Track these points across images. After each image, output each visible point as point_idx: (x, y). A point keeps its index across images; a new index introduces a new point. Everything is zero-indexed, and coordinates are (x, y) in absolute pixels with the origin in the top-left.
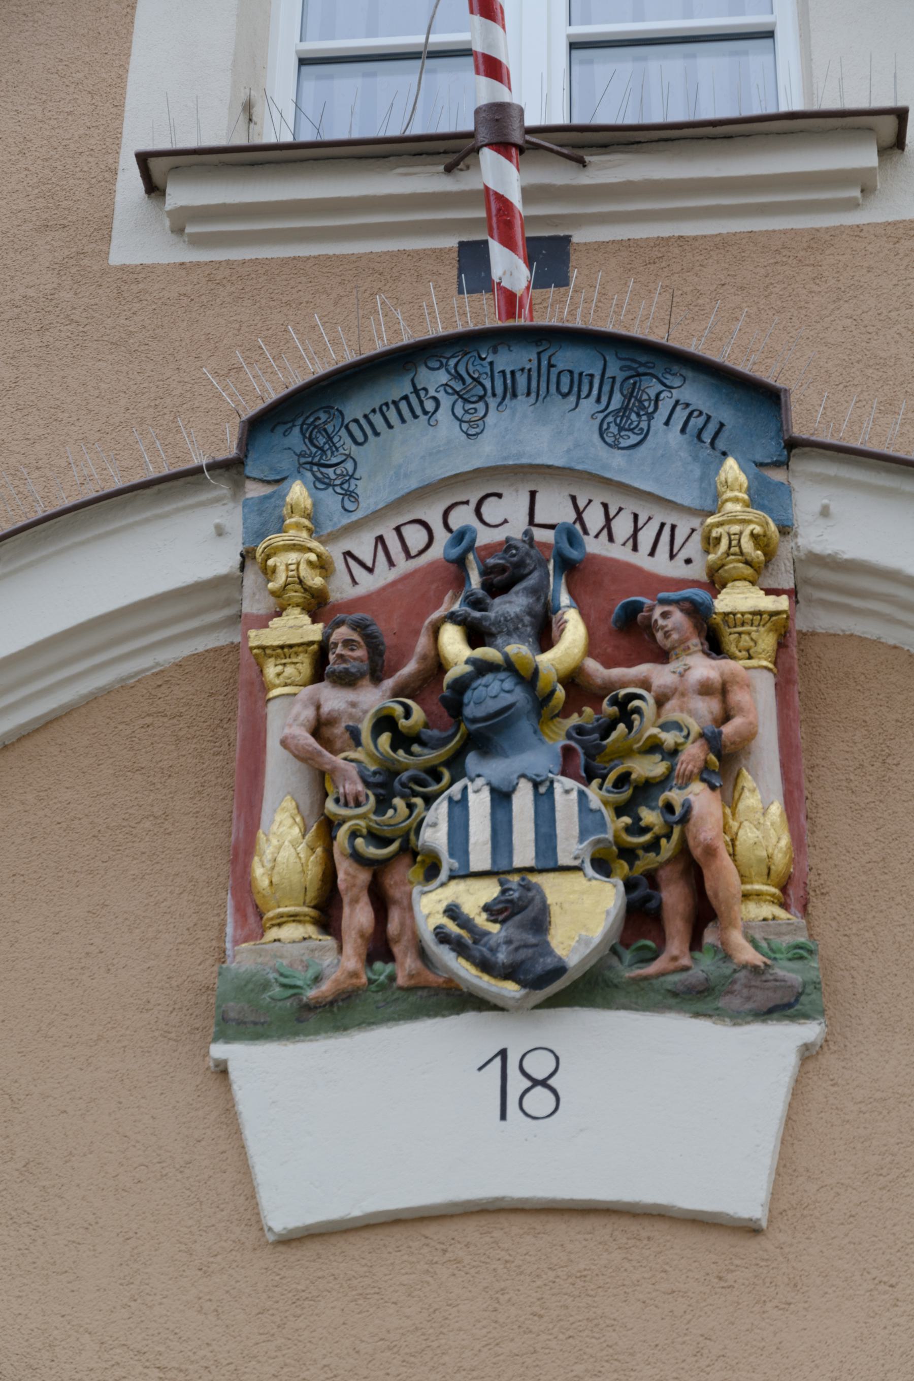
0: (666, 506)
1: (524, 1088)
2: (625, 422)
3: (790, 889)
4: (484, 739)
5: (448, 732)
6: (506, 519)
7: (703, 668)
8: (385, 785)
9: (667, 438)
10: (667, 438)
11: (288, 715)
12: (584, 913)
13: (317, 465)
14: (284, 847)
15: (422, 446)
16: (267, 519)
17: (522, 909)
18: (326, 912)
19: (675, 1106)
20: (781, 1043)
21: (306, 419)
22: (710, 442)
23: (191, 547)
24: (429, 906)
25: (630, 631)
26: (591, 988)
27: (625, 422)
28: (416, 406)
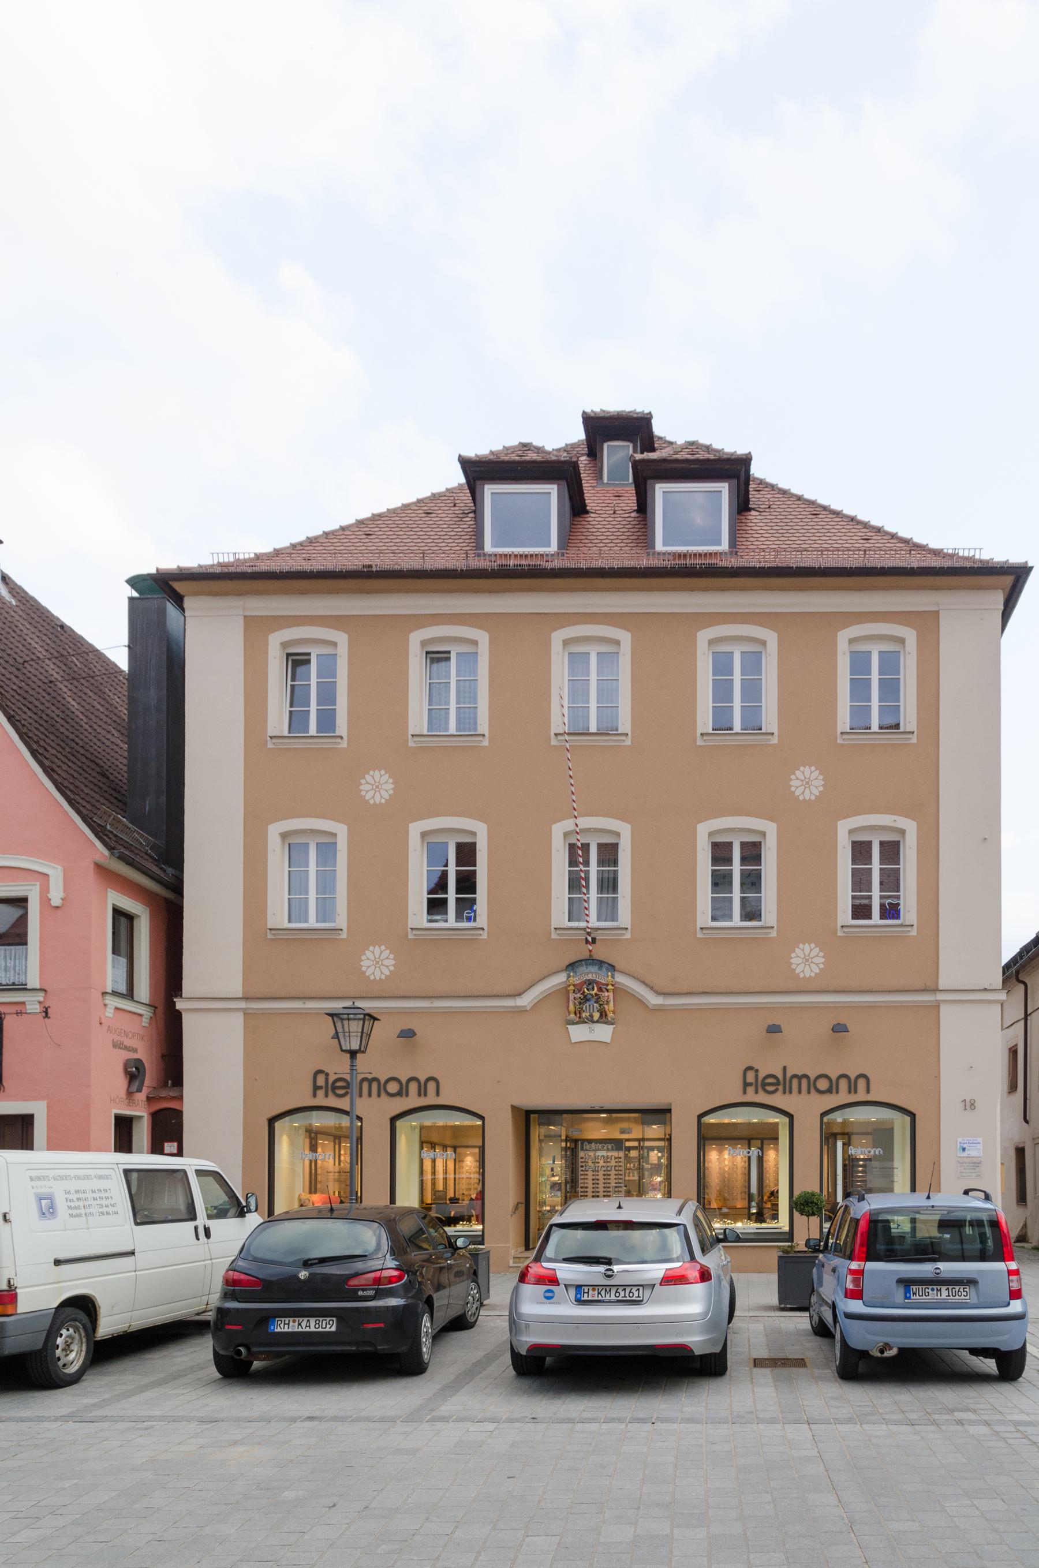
0: (602, 976)
1: (592, 1030)
2: (600, 968)
3: (614, 1012)
4: (588, 1000)
5: (586, 999)
6: (590, 977)
7: (606, 994)
8: (580, 1003)
9: (604, 970)
10: (604, 970)
11: (572, 996)
12: (596, 1016)
13: (573, 970)
14: (572, 1007)
15: (583, 969)
16: (569, 977)
17: (591, 1016)
18: (575, 1013)
19: (603, 1033)
20: (612, 1027)
21: (572, 966)
22: (608, 970)
23: (560, 979)
24: (584, 1015)
25: (600, 990)
26: (597, 1022)
27: (600, 968)
28: (582, 965)
